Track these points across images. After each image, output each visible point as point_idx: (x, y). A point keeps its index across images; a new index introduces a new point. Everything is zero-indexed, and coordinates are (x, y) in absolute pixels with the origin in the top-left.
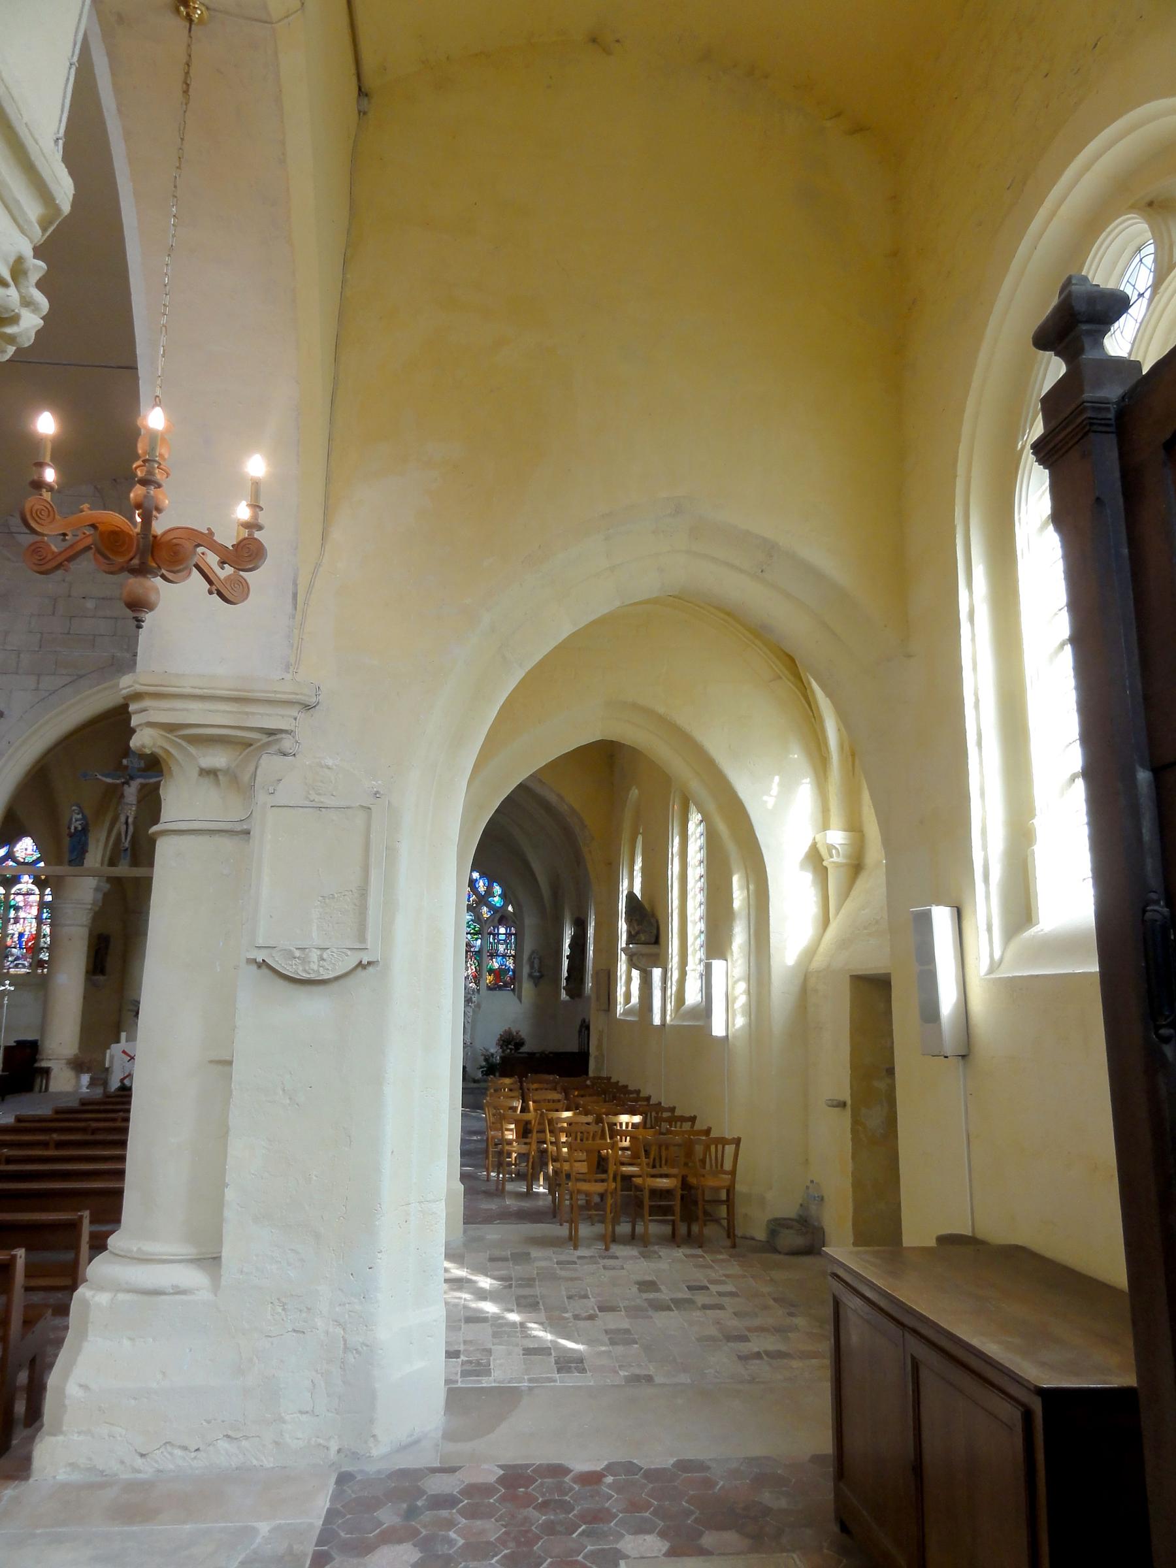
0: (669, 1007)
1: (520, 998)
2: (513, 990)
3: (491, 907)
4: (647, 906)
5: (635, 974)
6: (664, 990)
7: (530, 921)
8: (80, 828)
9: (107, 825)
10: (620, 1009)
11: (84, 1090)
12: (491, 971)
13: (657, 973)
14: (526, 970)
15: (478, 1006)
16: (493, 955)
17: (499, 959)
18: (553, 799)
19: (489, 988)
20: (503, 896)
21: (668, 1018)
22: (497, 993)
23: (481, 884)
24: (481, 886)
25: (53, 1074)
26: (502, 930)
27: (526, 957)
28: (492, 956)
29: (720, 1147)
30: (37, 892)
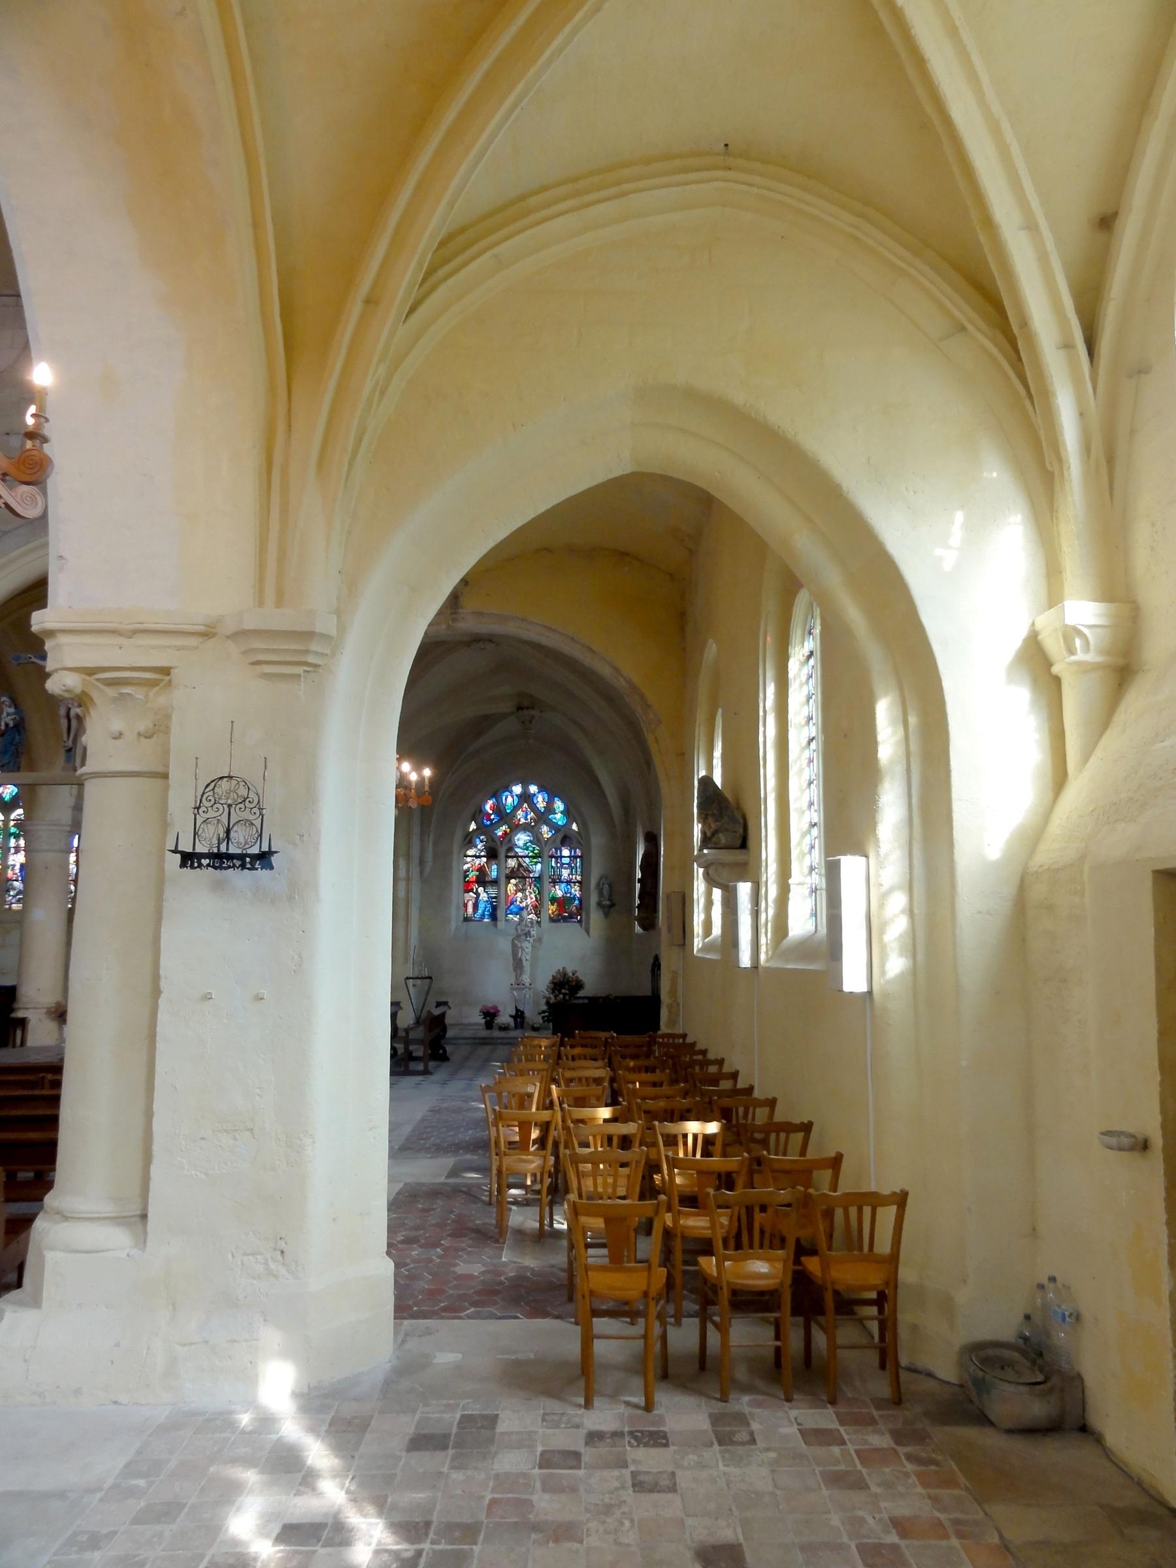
0: (763, 940)
1: (587, 931)
2: (580, 922)
3: (552, 826)
4: (728, 795)
5: (717, 893)
6: (756, 914)
7: (597, 841)
8: (11, 724)
10: (698, 943)
12: (554, 900)
13: (744, 889)
14: (594, 898)
15: (539, 940)
16: (556, 881)
17: (563, 885)
18: (606, 671)
19: (552, 920)
20: (566, 812)
21: (763, 957)
22: (562, 925)
23: (540, 798)
24: (541, 802)
26: (566, 852)
27: (593, 882)
29: (867, 1211)
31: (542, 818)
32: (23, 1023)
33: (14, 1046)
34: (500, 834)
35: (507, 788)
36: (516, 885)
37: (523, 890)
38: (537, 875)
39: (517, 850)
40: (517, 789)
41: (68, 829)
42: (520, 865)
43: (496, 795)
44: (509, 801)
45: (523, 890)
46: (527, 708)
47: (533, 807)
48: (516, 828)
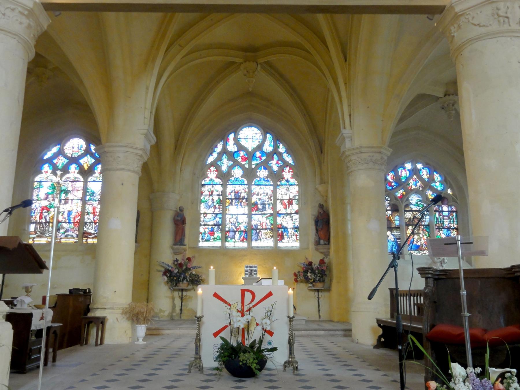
9: (156, 72)
11: (141, 342)
16: (440, 228)
17: (445, 231)
20: (445, 181)
24: (425, 174)
25: (108, 326)
26: (445, 208)
28: (439, 229)
30: (82, 180)
31: (427, 185)
33: (96, 345)
34: (399, 195)
37: (418, 234)
38: (427, 223)
39: (412, 206)
40: (408, 166)
41: (140, 152)
43: (395, 170)
44: (404, 174)
45: (418, 234)
46: (453, 95)
47: (420, 178)
48: (409, 192)
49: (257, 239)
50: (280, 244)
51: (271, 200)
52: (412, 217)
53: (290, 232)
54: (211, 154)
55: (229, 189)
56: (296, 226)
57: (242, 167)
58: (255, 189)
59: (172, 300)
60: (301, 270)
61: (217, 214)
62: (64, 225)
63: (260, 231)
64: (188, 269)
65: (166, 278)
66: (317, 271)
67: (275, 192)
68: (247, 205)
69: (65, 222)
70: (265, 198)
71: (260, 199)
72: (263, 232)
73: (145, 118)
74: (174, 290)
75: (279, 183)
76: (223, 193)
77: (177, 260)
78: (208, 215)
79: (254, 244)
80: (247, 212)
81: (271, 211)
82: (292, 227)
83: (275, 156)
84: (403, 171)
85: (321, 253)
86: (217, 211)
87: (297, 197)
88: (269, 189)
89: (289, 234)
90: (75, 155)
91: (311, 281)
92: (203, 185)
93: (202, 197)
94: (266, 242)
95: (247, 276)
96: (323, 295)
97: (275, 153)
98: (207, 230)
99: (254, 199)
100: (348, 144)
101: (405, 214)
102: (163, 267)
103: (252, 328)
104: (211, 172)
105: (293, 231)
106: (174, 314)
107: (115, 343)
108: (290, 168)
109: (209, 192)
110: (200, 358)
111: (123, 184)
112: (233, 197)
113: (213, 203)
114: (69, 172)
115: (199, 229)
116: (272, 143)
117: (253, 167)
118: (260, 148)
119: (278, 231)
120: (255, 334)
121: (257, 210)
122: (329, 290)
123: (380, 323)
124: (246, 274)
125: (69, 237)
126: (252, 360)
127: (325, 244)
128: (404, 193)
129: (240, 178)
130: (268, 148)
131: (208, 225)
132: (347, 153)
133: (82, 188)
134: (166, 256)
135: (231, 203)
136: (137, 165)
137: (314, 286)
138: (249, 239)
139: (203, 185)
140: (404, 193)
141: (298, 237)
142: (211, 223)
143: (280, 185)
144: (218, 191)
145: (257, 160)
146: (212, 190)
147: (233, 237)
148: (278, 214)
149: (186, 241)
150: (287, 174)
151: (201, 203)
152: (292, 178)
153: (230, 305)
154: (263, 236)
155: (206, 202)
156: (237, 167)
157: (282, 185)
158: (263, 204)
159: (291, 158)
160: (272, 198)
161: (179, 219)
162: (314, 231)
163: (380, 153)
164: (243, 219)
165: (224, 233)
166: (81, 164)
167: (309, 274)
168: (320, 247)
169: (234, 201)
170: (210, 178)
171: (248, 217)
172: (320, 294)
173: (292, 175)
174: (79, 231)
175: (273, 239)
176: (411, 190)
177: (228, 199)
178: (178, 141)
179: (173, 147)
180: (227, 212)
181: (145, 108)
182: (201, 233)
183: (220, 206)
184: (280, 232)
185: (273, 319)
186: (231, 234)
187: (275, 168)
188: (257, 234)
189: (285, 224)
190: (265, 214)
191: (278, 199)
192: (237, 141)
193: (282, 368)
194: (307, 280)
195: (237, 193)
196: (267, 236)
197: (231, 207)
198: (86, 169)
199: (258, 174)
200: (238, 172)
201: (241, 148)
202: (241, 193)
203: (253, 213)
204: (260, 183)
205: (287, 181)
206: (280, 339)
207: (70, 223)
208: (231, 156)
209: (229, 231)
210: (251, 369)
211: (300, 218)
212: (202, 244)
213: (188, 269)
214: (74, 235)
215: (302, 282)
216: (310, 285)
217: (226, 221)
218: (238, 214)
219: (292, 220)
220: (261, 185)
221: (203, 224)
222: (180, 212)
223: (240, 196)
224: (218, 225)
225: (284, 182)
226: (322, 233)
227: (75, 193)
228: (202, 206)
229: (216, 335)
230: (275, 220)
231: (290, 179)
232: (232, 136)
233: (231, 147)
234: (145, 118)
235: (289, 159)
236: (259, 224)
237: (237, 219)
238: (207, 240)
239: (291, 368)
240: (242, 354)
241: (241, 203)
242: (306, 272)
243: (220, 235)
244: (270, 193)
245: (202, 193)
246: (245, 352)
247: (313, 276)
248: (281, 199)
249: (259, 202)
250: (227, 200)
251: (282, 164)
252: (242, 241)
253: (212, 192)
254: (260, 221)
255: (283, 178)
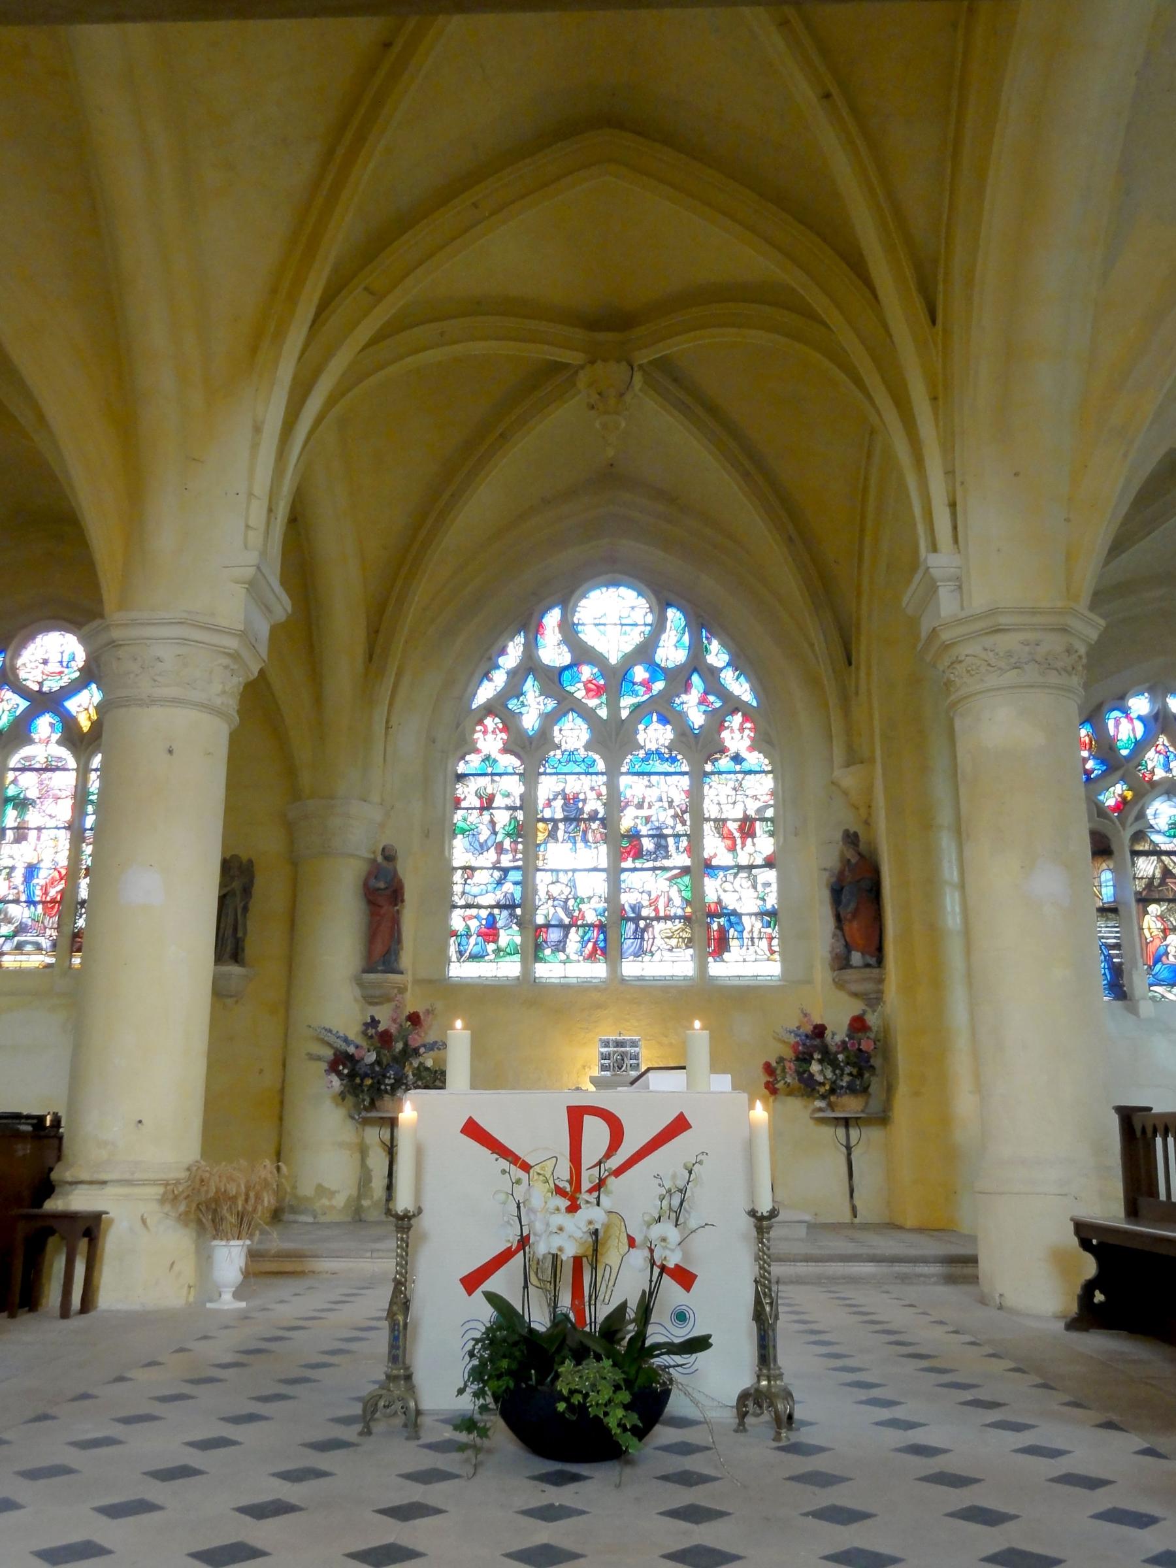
9: (286, 371)
11: (228, 1302)
25: (112, 1242)
30: (72, 763)
32: (89, 1229)
33: (65, 1313)
34: (1111, 802)
35: (1119, 702)
36: (1161, 917)
39: (1156, 838)
40: (1140, 705)
41: (232, 643)
42: (1166, 872)
43: (1094, 716)
44: (1125, 730)
49: (640, 953)
50: (716, 969)
51: (684, 823)
52: (1158, 875)
53: (748, 928)
54: (486, 676)
55: (547, 786)
56: (769, 906)
57: (588, 715)
58: (631, 787)
59: (357, 1156)
60: (789, 1054)
61: (506, 871)
62: (14, 910)
63: (647, 926)
64: (411, 1052)
65: (336, 1082)
66: (841, 1057)
67: (695, 796)
68: (606, 839)
69: (16, 901)
70: (665, 817)
71: (648, 820)
72: (658, 926)
73: (247, 526)
74: (366, 1122)
75: (708, 767)
76: (528, 802)
77: (374, 1022)
78: (477, 873)
79: (631, 968)
80: (604, 864)
81: (684, 860)
82: (756, 910)
83: (695, 679)
84: (1124, 721)
85: (855, 995)
86: (506, 860)
87: (769, 813)
88: (677, 788)
89: (745, 935)
90: (52, 685)
91: (822, 1090)
92: (461, 777)
93: (459, 815)
94: (668, 961)
95: (608, 1074)
96: (867, 1140)
97: (695, 670)
98: (474, 925)
99: (627, 821)
100: (947, 604)
101: (1133, 864)
102: (329, 1045)
103: (612, 1256)
104: (485, 732)
105: (758, 925)
106: (366, 1203)
107: (136, 1307)
108: (746, 718)
109: (481, 798)
110: (408, 1377)
111: (170, 752)
112: (559, 815)
113: (495, 833)
114: (30, 741)
115: (447, 918)
116: (686, 638)
117: (624, 714)
118: (645, 652)
119: (709, 925)
120: (623, 1282)
121: (638, 854)
122: (883, 1119)
123: (1087, 1235)
124: (604, 1068)
125: (29, 948)
126: (606, 1393)
127: (868, 966)
128: (1129, 795)
129: (582, 752)
130: (672, 651)
131: (479, 907)
132: (945, 636)
133: (70, 791)
134: (337, 1005)
135: (552, 835)
136: (221, 686)
137: (831, 1106)
138: (612, 952)
139: (461, 777)
140: (1129, 795)
141: (775, 942)
142: (489, 900)
143: (713, 773)
144: (508, 795)
145: (634, 693)
146: (489, 791)
147: (560, 946)
148: (708, 867)
149: (406, 959)
150: (737, 737)
151: (454, 836)
152: (751, 749)
153: (526, 1167)
154: (659, 942)
155: (470, 832)
156: (570, 716)
157: (720, 773)
158: (659, 837)
159: (747, 686)
160: (687, 816)
161: (382, 885)
162: (830, 924)
163: (1064, 630)
164: (594, 886)
165: (531, 933)
166: (68, 712)
167: (815, 1068)
168: (849, 974)
169: (561, 826)
170: (485, 752)
171: (608, 880)
172: (854, 1133)
173: (753, 739)
174: (58, 928)
175: (691, 951)
176: (1153, 784)
177: (544, 820)
178: (377, 632)
179: (360, 650)
180: (540, 864)
181: (250, 495)
182: (455, 934)
183: (516, 842)
184: (715, 926)
185: (693, 1223)
186: (554, 935)
187: (697, 718)
188: (640, 934)
189: (730, 902)
190: (664, 869)
191: (708, 820)
192: (569, 632)
193: (729, 1417)
194: (808, 1087)
195: (571, 803)
196: (673, 942)
197: (551, 845)
198: (85, 729)
199: (641, 738)
200: (576, 733)
201: (583, 654)
202: (584, 801)
203: (624, 865)
204: (647, 769)
205: (737, 759)
206: (720, 1305)
207: (30, 902)
208: (552, 680)
209: (548, 926)
210: (608, 1430)
211: (781, 880)
212: (459, 970)
213: (411, 1052)
214: (45, 943)
215: (791, 1093)
216: (819, 1104)
217: (535, 892)
218: (574, 871)
219: (755, 887)
220: (649, 774)
221: (462, 902)
222: (385, 864)
223: (581, 811)
224: (510, 906)
225: (724, 763)
226: (854, 928)
227: (49, 806)
228: (459, 843)
229: (471, 1282)
230: (698, 890)
231: (744, 754)
232: (552, 618)
233: (553, 652)
234: (247, 526)
235: (741, 688)
236: (645, 903)
237: (572, 884)
238: (475, 957)
239: (767, 1416)
240: (567, 1367)
241: (585, 832)
242: (804, 1059)
243: (518, 940)
244: (680, 799)
245: (458, 801)
246: (580, 1354)
247: (829, 1074)
248: (716, 820)
249: (644, 830)
250: (541, 825)
251: (718, 704)
252: (591, 957)
253: (491, 799)
254: (649, 894)
255: (723, 750)
